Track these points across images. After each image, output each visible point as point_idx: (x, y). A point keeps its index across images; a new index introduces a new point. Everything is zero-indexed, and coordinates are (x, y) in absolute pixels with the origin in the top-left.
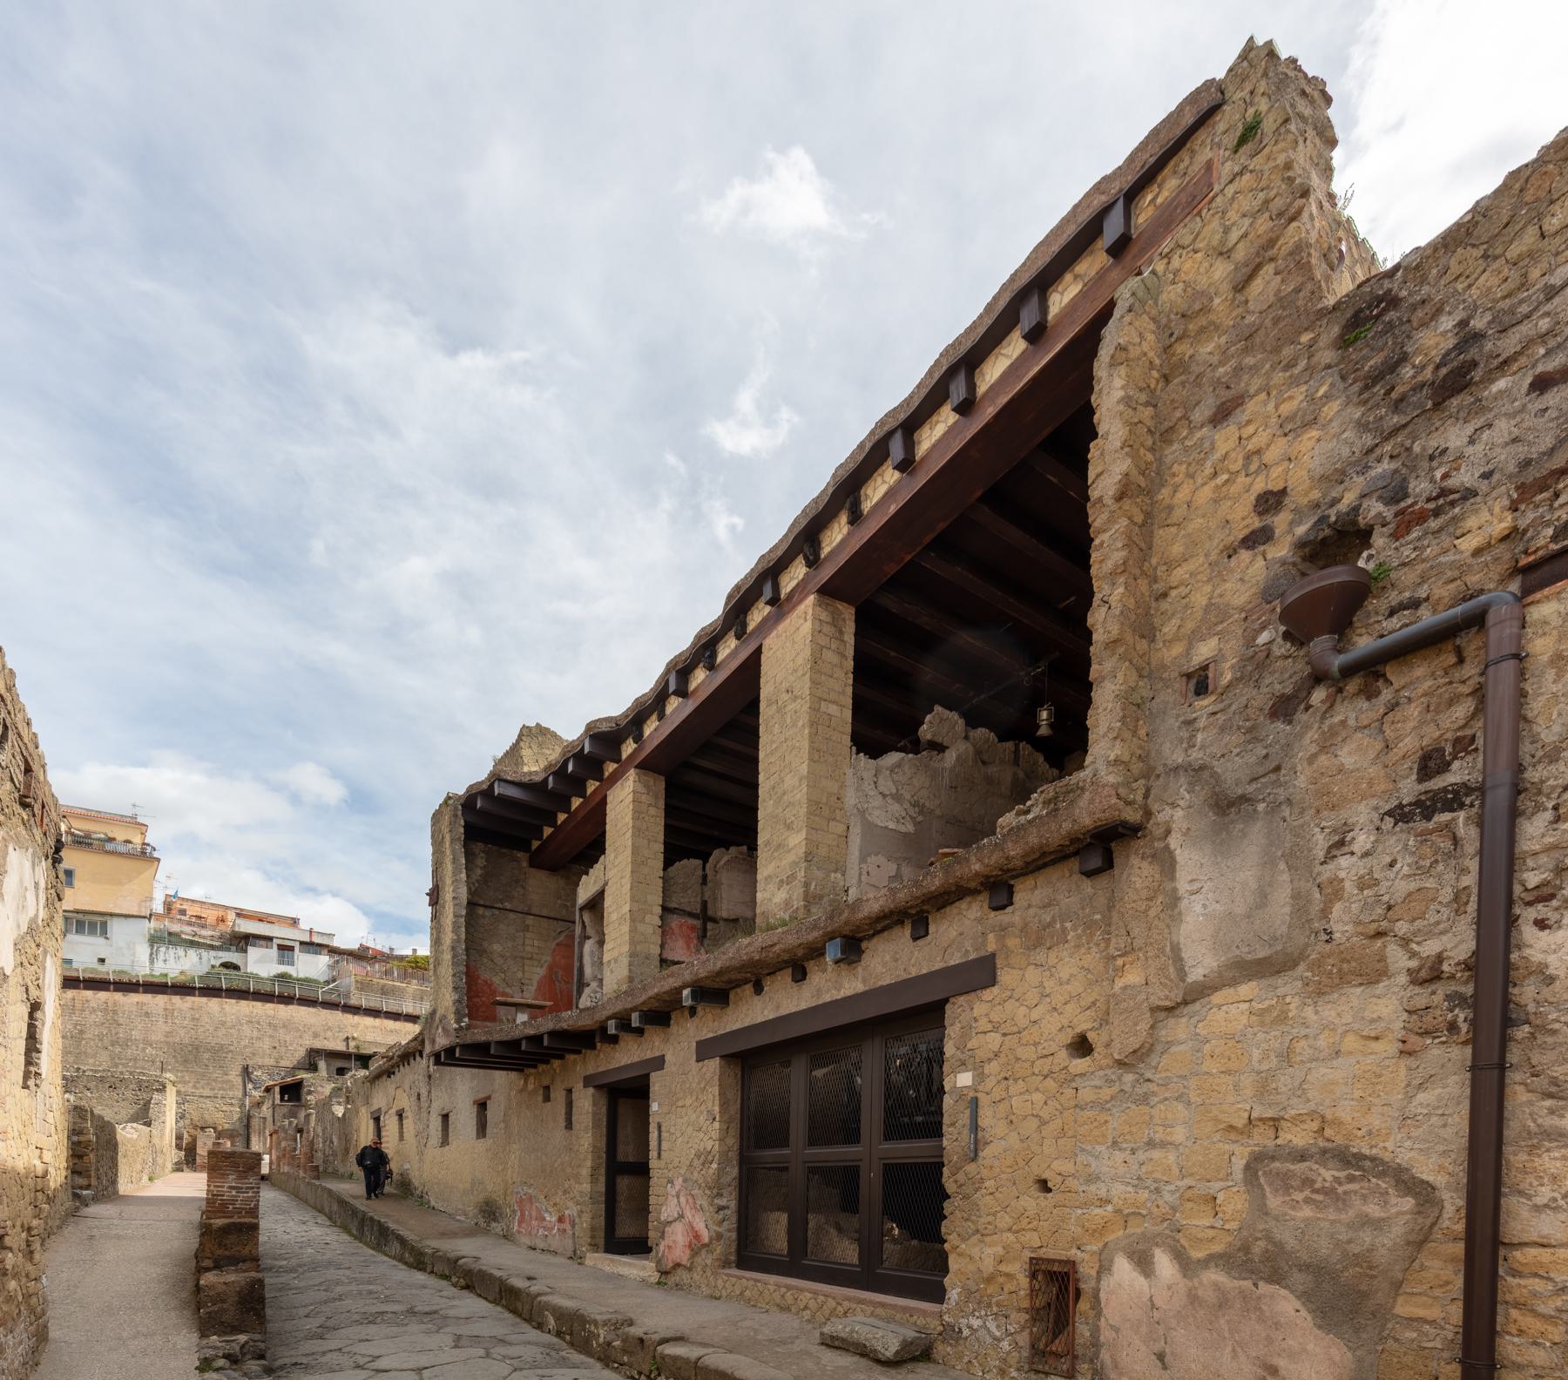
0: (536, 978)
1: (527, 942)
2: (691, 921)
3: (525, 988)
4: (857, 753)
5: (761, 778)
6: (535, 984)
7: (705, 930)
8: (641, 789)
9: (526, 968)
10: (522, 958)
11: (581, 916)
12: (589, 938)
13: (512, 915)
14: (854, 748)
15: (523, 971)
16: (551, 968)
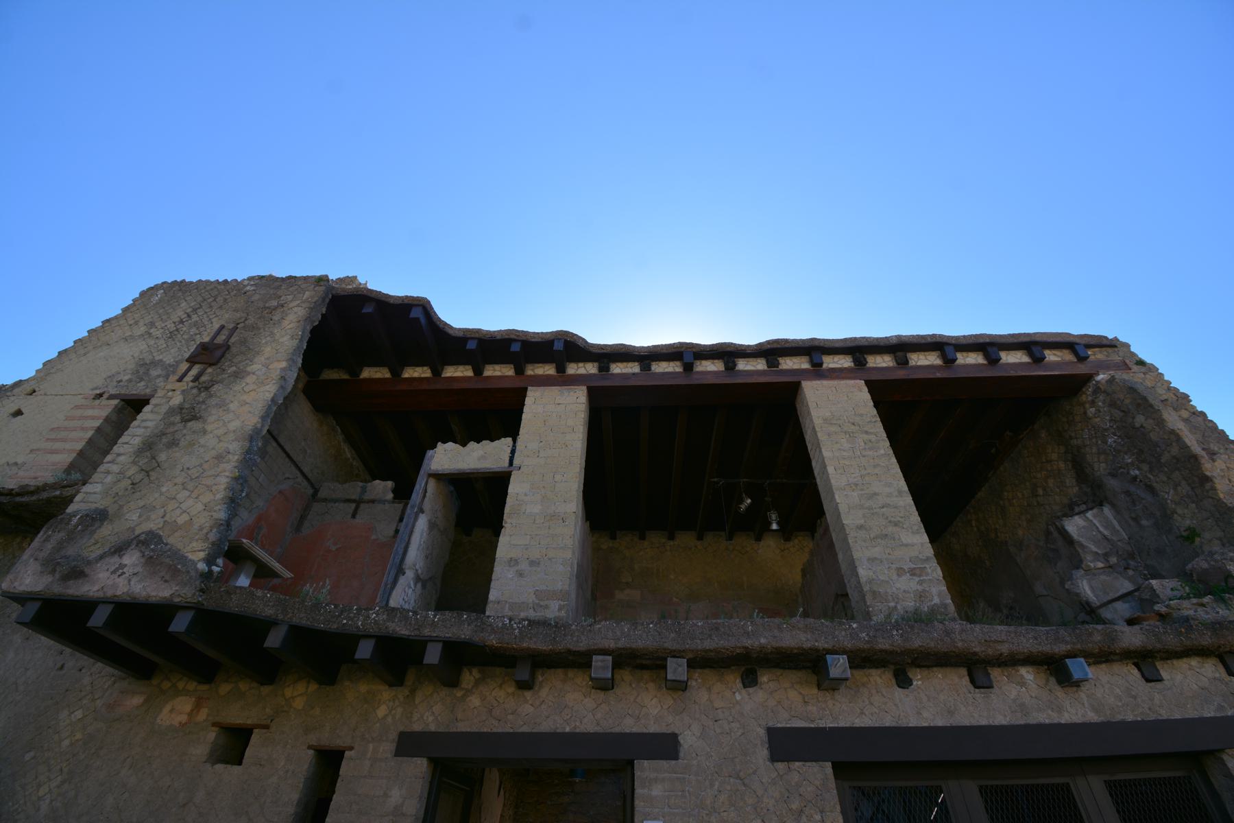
12: (423, 512)
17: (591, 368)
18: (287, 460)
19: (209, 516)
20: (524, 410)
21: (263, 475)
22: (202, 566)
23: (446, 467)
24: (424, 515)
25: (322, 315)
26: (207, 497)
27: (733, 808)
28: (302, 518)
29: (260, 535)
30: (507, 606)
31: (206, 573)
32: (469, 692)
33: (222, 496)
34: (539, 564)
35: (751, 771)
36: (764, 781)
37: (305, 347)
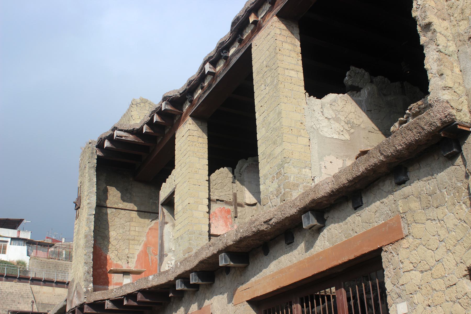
0: (137, 253)
1: (132, 229)
2: (227, 207)
3: (130, 260)
4: (310, 96)
5: (257, 115)
6: (136, 257)
7: (236, 212)
9: (131, 246)
10: (128, 239)
12: (167, 223)
14: (307, 94)
16: (146, 246)
18: (146, 213)
20: (176, 149)
22: (85, 290)
25: (97, 159)
29: (151, 251)
37: (96, 180)
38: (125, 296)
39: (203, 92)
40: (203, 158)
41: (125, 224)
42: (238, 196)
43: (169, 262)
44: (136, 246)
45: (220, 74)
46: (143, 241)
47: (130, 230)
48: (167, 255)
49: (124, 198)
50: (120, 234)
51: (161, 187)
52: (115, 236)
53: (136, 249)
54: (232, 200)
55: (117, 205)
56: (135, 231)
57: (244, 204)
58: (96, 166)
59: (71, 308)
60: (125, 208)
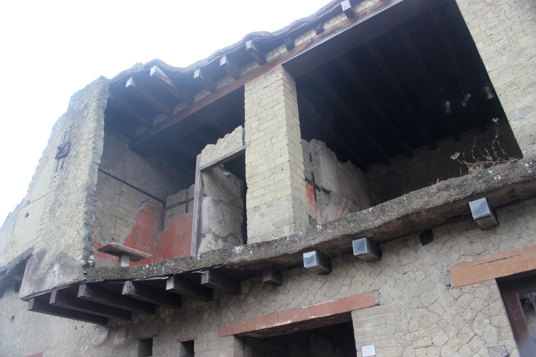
1: (121, 204)
8: (285, 78)
10: (115, 216)
11: (201, 177)
12: (205, 196)
13: (113, 181)
15: (115, 228)
16: (135, 229)
17: (283, 50)
18: (138, 192)
19: (80, 236)
20: (245, 102)
21: (126, 205)
22: (83, 262)
23: (209, 162)
24: (207, 197)
25: (108, 100)
26: (78, 227)
27: (422, 328)
28: (163, 222)
29: (140, 238)
30: (259, 238)
31: (85, 265)
32: (247, 295)
33: (82, 224)
34: (272, 205)
35: (433, 301)
36: (443, 305)
37: (103, 124)
38: (170, 276)
39: (318, 36)
40: (295, 116)
41: (114, 197)
42: (315, 177)
43: (208, 245)
44: (123, 227)
45: (365, 14)
46: (131, 223)
47: (118, 205)
48: (204, 237)
49: (117, 164)
50: (107, 207)
51: (203, 149)
52: (100, 207)
53: (123, 232)
54: (311, 179)
55: (108, 170)
56: (124, 208)
57: (320, 188)
58: (106, 107)
59: (37, 291)
60: (116, 176)
